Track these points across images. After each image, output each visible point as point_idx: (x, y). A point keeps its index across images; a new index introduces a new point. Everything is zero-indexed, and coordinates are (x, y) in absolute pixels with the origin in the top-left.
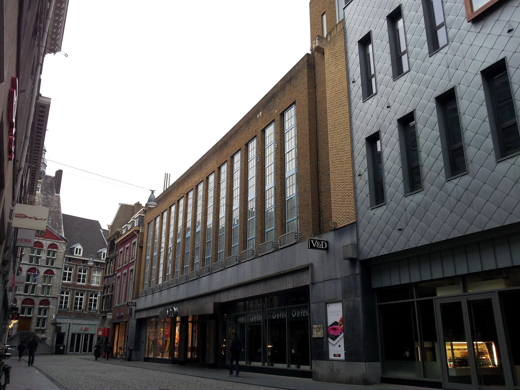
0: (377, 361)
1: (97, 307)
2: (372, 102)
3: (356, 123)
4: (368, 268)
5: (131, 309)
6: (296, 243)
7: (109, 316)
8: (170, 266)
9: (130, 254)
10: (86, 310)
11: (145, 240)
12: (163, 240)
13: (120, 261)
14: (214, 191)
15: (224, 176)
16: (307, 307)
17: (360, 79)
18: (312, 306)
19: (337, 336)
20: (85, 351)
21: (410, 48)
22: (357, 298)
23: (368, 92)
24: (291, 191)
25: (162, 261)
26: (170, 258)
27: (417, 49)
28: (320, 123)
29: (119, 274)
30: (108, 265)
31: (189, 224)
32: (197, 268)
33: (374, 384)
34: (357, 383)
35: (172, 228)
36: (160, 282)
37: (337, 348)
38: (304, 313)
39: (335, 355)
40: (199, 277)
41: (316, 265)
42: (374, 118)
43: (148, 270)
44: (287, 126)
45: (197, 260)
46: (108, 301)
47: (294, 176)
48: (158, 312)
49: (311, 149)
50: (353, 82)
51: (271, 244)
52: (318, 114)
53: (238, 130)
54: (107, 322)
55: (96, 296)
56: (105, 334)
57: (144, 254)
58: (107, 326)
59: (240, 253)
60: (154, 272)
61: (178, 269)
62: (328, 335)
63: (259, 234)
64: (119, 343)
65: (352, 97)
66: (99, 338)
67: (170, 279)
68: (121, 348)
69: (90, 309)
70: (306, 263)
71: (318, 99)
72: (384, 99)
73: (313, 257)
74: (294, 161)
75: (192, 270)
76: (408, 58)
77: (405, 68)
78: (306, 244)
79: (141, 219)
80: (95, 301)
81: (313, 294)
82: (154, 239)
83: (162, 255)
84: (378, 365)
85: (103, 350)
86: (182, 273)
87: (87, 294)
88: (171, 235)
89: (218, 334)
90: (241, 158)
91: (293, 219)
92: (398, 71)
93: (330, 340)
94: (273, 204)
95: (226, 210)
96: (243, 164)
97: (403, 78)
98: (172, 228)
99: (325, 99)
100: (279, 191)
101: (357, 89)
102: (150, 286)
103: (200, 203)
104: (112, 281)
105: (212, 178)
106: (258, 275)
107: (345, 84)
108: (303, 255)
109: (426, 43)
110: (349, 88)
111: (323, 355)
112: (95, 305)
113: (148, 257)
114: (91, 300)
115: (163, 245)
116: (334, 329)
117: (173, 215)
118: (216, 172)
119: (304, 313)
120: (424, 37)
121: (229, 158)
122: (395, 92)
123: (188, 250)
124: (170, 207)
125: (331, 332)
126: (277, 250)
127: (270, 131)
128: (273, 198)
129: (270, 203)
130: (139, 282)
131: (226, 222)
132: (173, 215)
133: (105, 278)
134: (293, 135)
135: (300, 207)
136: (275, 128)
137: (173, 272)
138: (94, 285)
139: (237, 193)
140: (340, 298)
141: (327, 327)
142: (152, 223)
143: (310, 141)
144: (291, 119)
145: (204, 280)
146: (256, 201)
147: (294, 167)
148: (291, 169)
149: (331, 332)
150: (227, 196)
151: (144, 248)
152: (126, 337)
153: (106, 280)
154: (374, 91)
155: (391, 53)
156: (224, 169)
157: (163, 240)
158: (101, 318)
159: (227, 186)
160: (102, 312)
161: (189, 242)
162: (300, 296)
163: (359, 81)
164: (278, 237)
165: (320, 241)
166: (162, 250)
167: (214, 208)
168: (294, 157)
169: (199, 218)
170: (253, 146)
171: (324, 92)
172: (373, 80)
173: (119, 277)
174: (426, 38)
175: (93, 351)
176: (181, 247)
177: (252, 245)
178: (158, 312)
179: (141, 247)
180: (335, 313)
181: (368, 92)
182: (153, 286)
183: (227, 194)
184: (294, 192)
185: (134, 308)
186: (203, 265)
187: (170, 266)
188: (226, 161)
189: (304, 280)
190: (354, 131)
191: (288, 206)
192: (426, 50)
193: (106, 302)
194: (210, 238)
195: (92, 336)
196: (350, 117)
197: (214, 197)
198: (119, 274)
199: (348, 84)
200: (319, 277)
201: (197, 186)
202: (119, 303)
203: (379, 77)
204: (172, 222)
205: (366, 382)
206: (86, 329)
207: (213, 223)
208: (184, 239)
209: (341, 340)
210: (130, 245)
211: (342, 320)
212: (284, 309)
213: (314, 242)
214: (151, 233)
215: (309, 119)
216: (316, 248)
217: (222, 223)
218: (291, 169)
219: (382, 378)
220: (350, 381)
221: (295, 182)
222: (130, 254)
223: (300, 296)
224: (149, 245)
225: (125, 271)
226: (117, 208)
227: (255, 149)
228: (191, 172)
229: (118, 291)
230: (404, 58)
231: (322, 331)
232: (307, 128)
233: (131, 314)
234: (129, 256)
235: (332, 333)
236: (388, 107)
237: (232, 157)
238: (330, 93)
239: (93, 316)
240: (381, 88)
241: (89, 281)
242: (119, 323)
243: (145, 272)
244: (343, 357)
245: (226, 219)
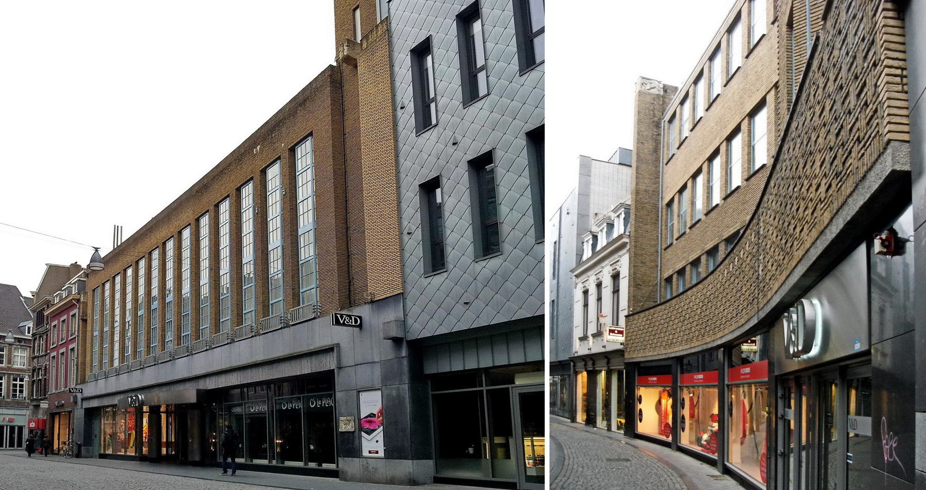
0: (428, 457)
1: (25, 394)
2: (430, 136)
3: (405, 164)
4: (420, 350)
5: (75, 397)
6: (314, 318)
7: (44, 405)
8: (129, 344)
9: (68, 328)
10: (8, 397)
11: (89, 312)
12: (117, 312)
13: (54, 337)
14: (191, 250)
15: (205, 231)
16: (332, 396)
17: (412, 104)
18: (339, 395)
19: (374, 430)
20: (12, 445)
21: (491, 62)
22: (403, 386)
23: (424, 122)
24: (307, 251)
25: (117, 338)
26: (129, 334)
27: (502, 64)
28: (350, 163)
29: (54, 354)
30: (37, 342)
31: (155, 292)
32: (170, 347)
33: (424, 484)
34: (401, 483)
35: (129, 297)
36: (116, 363)
37: (373, 444)
38: (326, 402)
39: (370, 452)
40: (173, 358)
41: (342, 345)
42: (432, 159)
43: (96, 348)
44: (300, 165)
45: (170, 336)
46: (41, 387)
47: (312, 233)
48: (115, 400)
49: (336, 197)
50: (402, 108)
51: (278, 319)
52: (348, 151)
53: (225, 169)
54: (41, 412)
55: (22, 380)
56: (40, 426)
57: (89, 328)
58: (41, 416)
59: (232, 330)
60: (106, 352)
61: (142, 348)
62: (361, 429)
63: (260, 306)
64: (61, 435)
65: (400, 128)
66: (31, 431)
67: (131, 360)
68: (65, 443)
69: (14, 396)
70: (330, 343)
71: (347, 131)
72: (448, 133)
73: (341, 335)
74: (311, 213)
75: (163, 349)
76: (487, 77)
77: (482, 91)
78: (329, 319)
79: (82, 286)
80: (21, 386)
81: (340, 381)
82: (102, 311)
83: (117, 330)
84: (431, 463)
85: (40, 443)
86: (148, 353)
87: (9, 378)
88: (129, 306)
89: (201, 427)
90: (230, 207)
91: (310, 289)
92: (471, 94)
93: (363, 434)
94: (280, 268)
95: (210, 275)
96: (234, 215)
97: (479, 104)
98: (129, 297)
99: (358, 130)
100: (288, 252)
101: (407, 118)
102: (101, 369)
103: (170, 265)
104: (44, 362)
105: (186, 234)
106: (260, 358)
107: (389, 110)
108: (324, 333)
109: (516, 56)
110: (395, 116)
111: (354, 451)
112: (21, 391)
113: (96, 333)
114: (15, 385)
115: (117, 318)
116: (370, 422)
117: (129, 280)
118: (193, 226)
119: (326, 402)
120: (513, 47)
121: (212, 208)
122: (466, 123)
123: (156, 323)
124: (125, 270)
125: (366, 425)
126: (288, 326)
127: (274, 173)
128: (280, 261)
129: (276, 266)
130: (84, 363)
131: (210, 291)
132: (129, 280)
133: (33, 358)
134: (309, 178)
135: (320, 273)
136: (282, 168)
137: (135, 352)
138: (17, 366)
139: (225, 253)
140: (377, 386)
141: (360, 420)
142: (99, 290)
143: (336, 187)
144: (305, 156)
145: (181, 363)
146: (255, 265)
147: (311, 220)
148: (306, 223)
149: (366, 425)
150: (210, 257)
151: (89, 321)
152: (71, 431)
153: (35, 360)
154: (434, 122)
155: (461, 68)
156: (205, 221)
157: (117, 312)
158: (31, 407)
159: (210, 243)
160: (32, 400)
161: (157, 316)
162: (324, 382)
163: (411, 107)
164: (288, 310)
165: (350, 316)
166: (116, 324)
167: (191, 273)
168: (310, 207)
169: (170, 284)
170: (248, 192)
171: (357, 120)
172: (433, 105)
173: (54, 357)
174: (516, 49)
175: (24, 445)
176: (145, 321)
177: (250, 320)
178: (115, 400)
179: (85, 321)
180: (371, 403)
181: (424, 122)
182: (106, 368)
183: (210, 254)
184: (312, 253)
185: (79, 396)
186: (179, 344)
187: (129, 344)
188: (208, 211)
189: (328, 363)
190: (402, 176)
191: (303, 272)
192: (515, 66)
193: (37, 387)
194: (188, 309)
195: (21, 428)
196: (397, 156)
197: (191, 259)
198: (54, 354)
199: (394, 110)
200: (347, 360)
201: (164, 244)
202: (56, 389)
203: (442, 102)
204: (129, 289)
205: (413, 482)
206: (11, 420)
207: (191, 291)
208: (149, 310)
209: (379, 434)
210: (68, 317)
211: (381, 412)
212: (299, 398)
213: (342, 317)
214: (98, 303)
215: (334, 157)
216: (344, 324)
217: (205, 291)
218: (306, 223)
219: (434, 478)
220: (392, 481)
221: (312, 240)
222: (68, 328)
223: (324, 382)
224: (97, 317)
225: (63, 350)
226: (41, 272)
227: (251, 196)
228: (155, 225)
229: (54, 374)
230: (481, 77)
231: (352, 423)
232: (330, 169)
233: (76, 403)
234: (68, 331)
235: (367, 426)
236: (454, 144)
237: (217, 206)
238: (365, 123)
239: (20, 405)
240: (444, 118)
241: (9, 362)
242: (59, 414)
243: (92, 352)
244: (381, 454)
245: (210, 286)
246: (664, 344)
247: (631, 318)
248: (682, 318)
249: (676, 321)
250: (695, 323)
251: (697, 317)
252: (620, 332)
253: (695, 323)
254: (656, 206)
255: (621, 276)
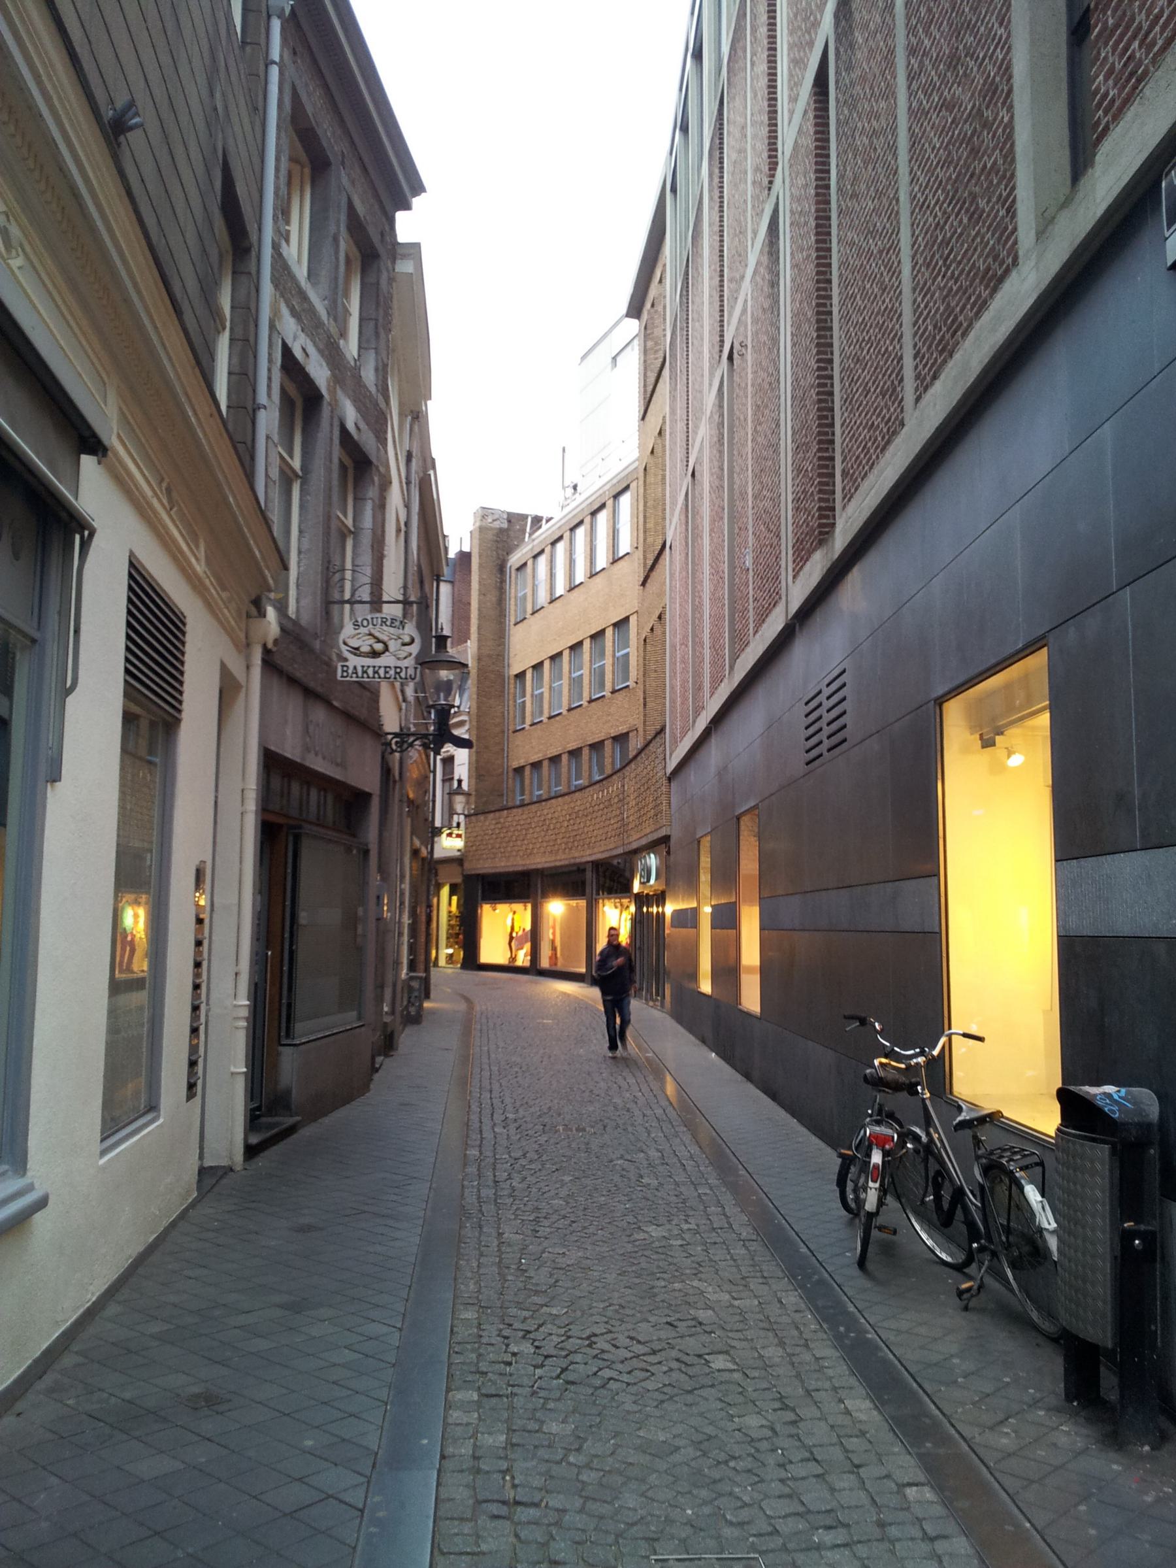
246: (521, 853)
247: (473, 818)
248: (545, 828)
249: (538, 829)
250: (561, 836)
251: (563, 830)
252: (459, 836)
253: (561, 836)
254: (501, 676)
255: (456, 762)
